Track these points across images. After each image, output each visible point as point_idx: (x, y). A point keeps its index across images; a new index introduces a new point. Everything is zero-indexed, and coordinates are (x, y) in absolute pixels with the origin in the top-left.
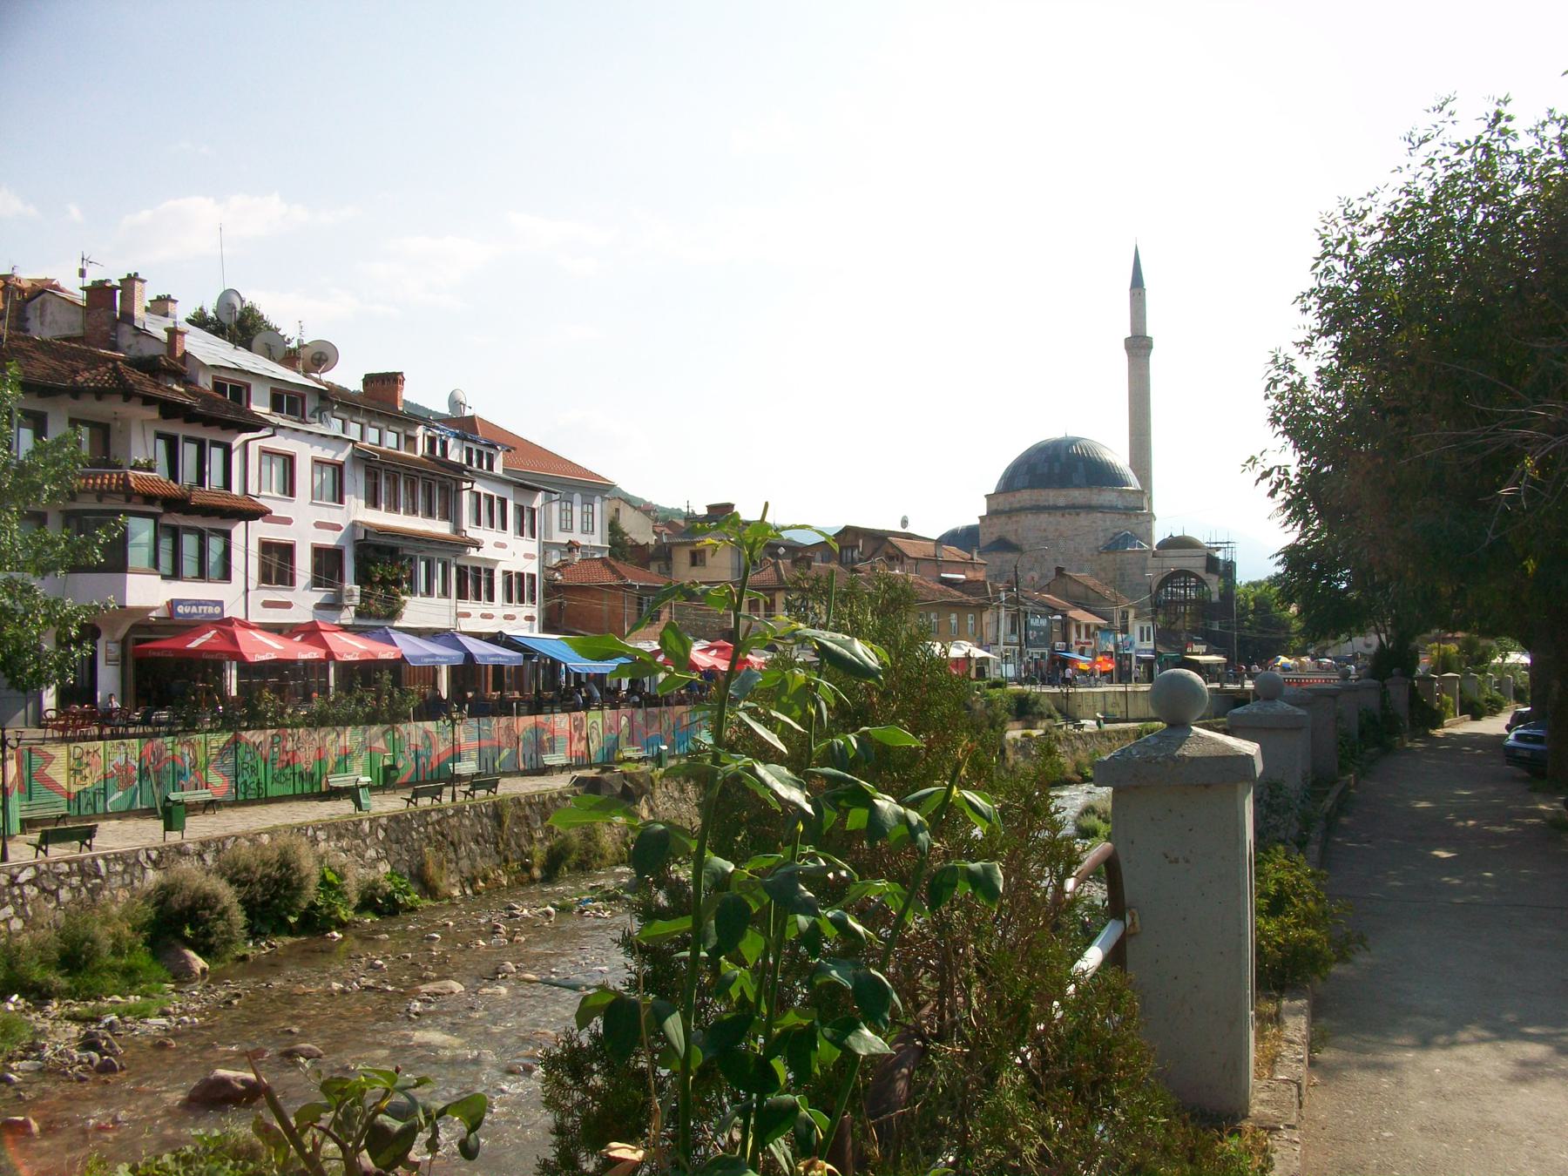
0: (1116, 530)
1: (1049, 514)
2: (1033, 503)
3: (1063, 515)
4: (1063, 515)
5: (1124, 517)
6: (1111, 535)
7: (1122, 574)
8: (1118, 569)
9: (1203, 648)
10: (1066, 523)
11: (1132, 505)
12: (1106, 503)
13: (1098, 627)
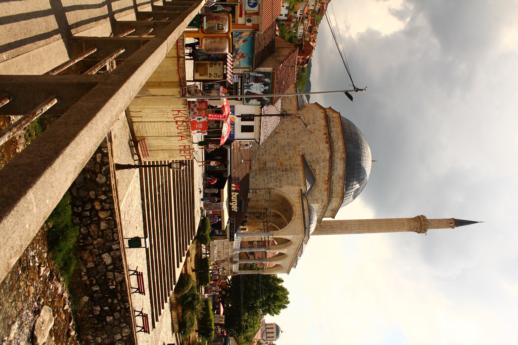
0: (317, 172)
1: (325, 126)
2: (331, 119)
3: (325, 134)
4: (325, 134)
5: (327, 179)
6: (313, 167)
7: (287, 170)
8: (291, 168)
9: (235, 208)
10: (321, 134)
11: (334, 188)
12: (335, 164)
13: (256, 28)
